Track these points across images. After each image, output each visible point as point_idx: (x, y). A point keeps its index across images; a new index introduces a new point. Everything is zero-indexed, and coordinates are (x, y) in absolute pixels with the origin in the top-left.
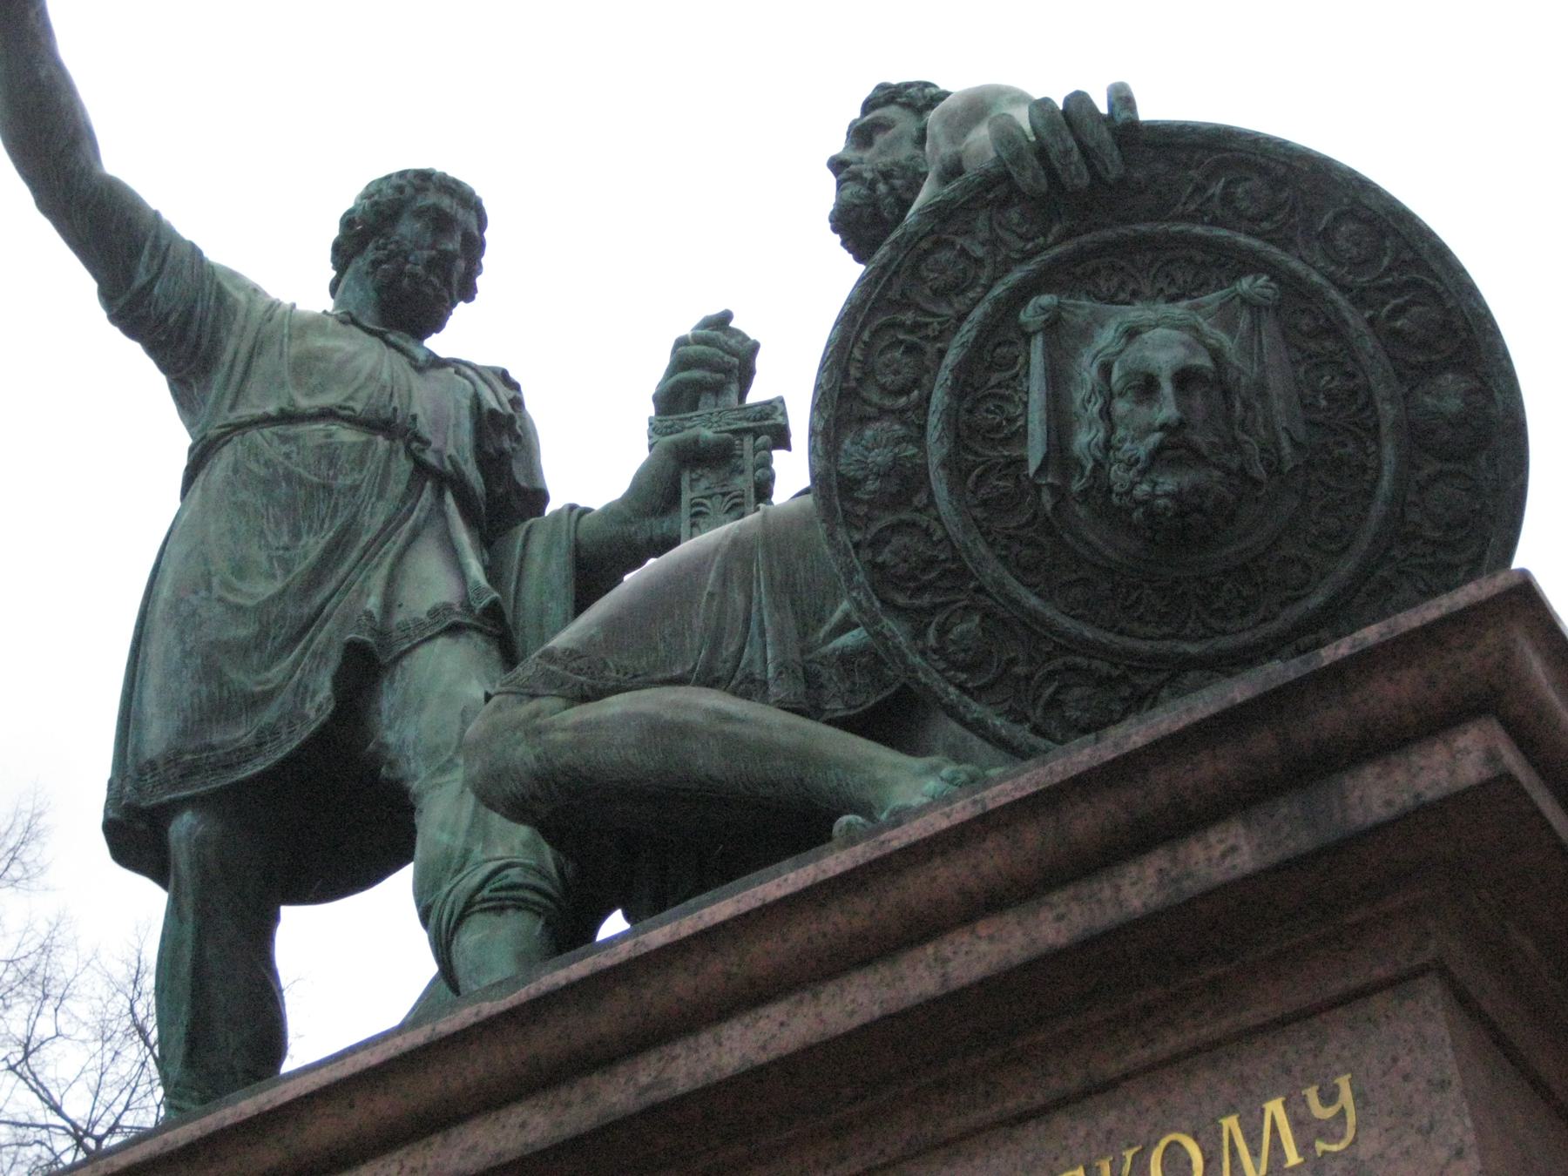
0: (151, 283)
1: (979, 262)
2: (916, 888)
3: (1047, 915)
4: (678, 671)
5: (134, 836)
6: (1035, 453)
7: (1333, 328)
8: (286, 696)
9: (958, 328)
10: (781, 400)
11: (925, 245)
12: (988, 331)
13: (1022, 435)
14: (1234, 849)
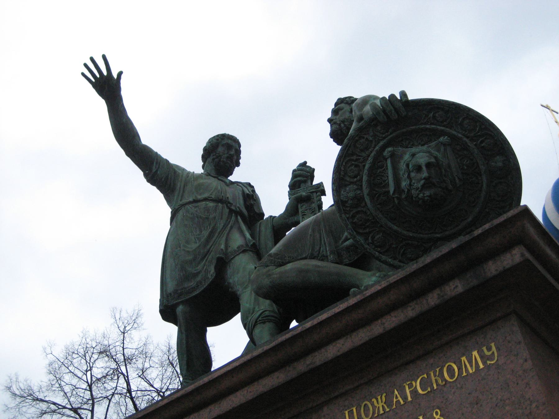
0: (157, 171)
1: (371, 141)
3: (409, 309)
4: (304, 256)
5: (168, 313)
6: (392, 189)
9: (368, 159)
10: (322, 183)
11: (357, 138)
12: (375, 158)
13: (388, 185)
14: (457, 286)
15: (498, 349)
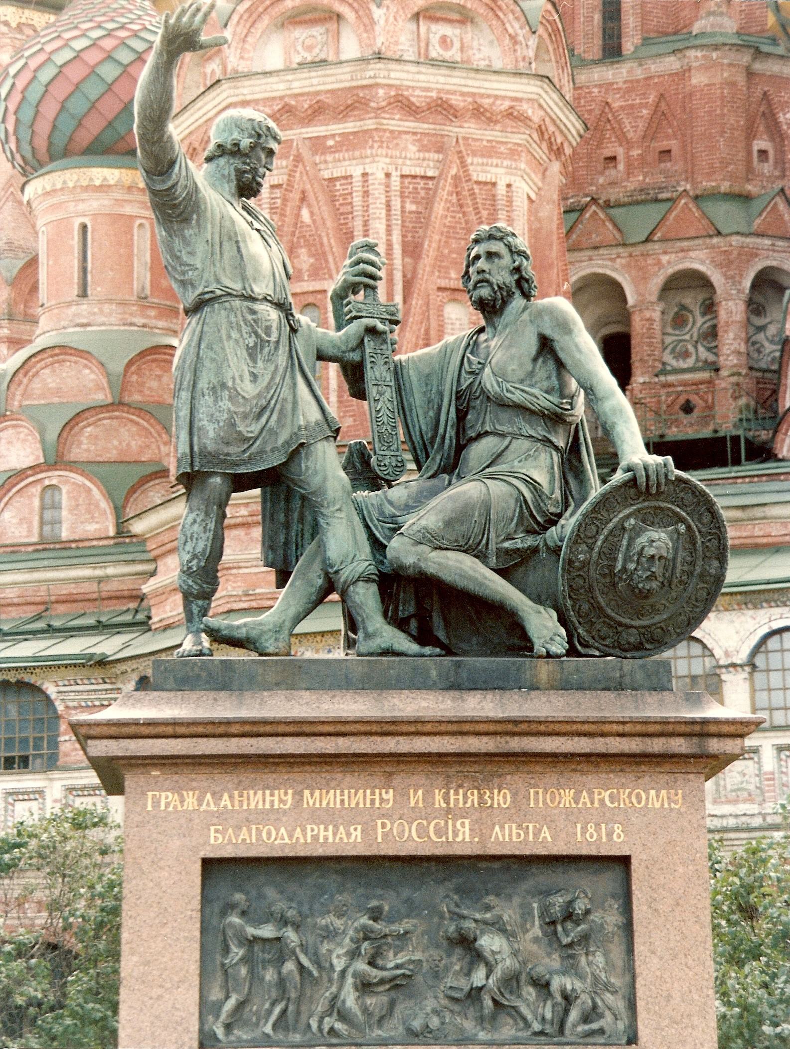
2: (607, 728)
6: (619, 566)
7: (693, 542)
15: (684, 798)
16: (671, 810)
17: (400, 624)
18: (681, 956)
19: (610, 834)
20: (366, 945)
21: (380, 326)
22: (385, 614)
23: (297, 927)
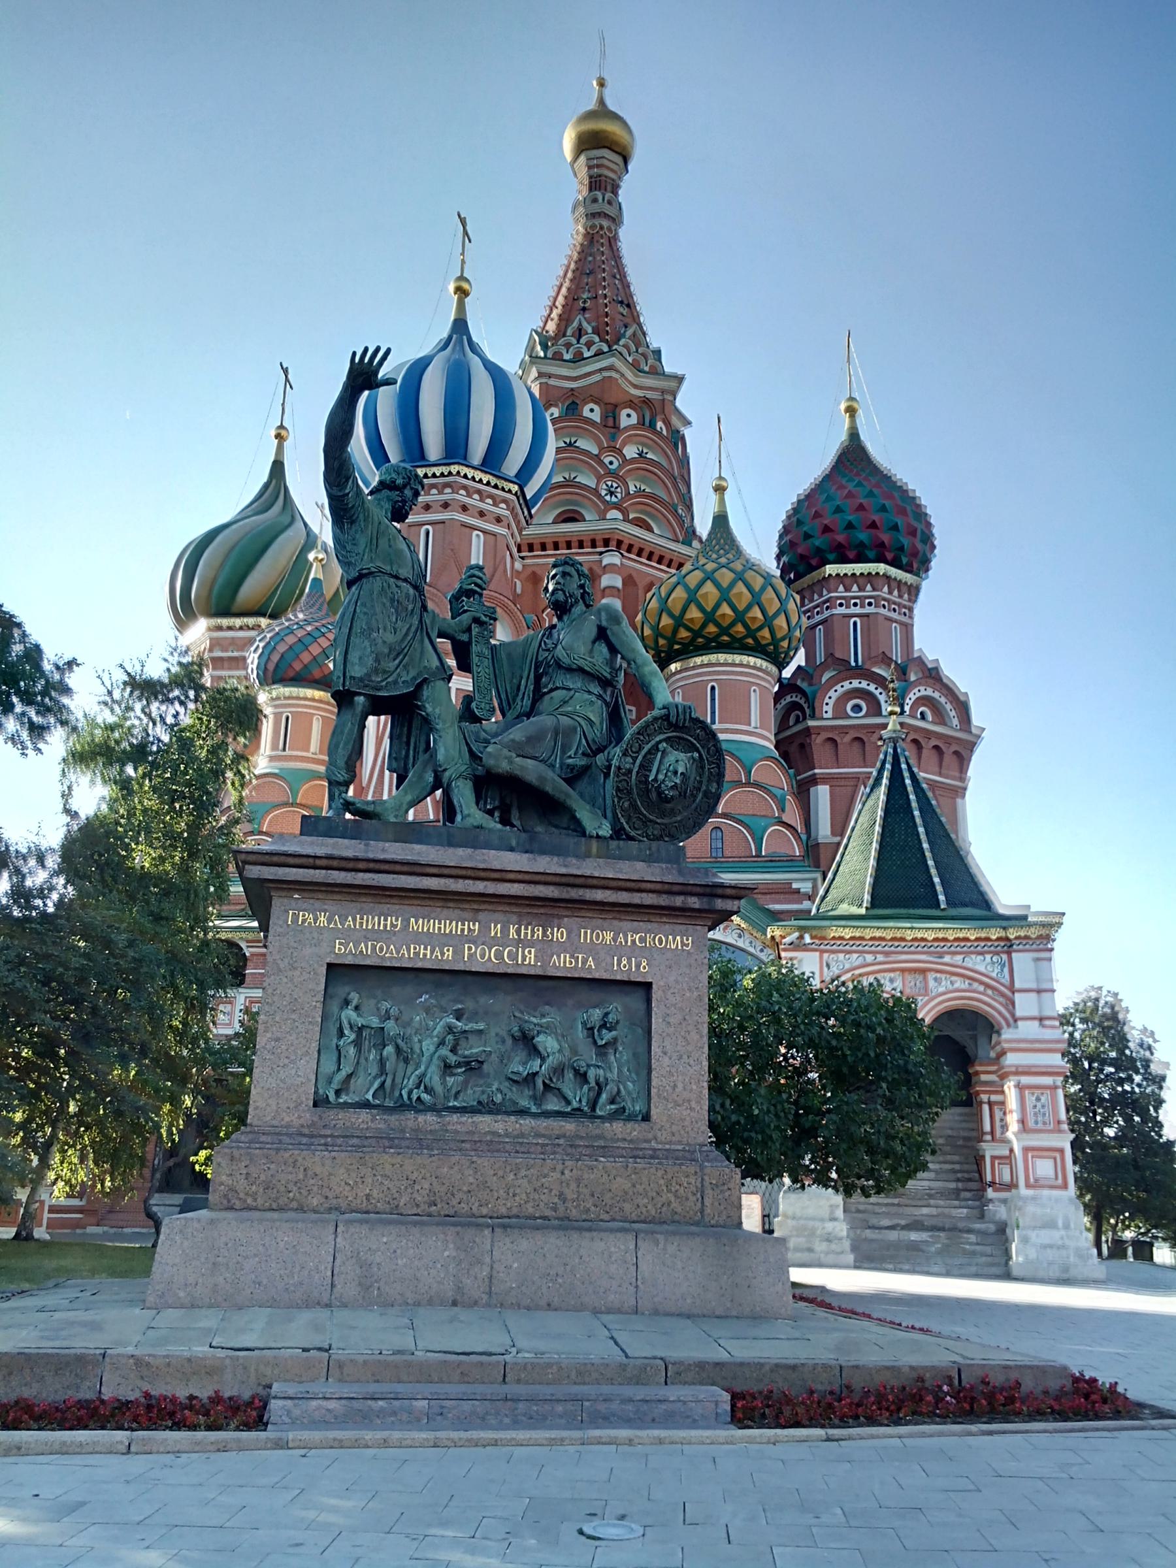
2: (644, 886)
7: (703, 768)
8: (395, 675)
16: (683, 950)
17: (490, 813)
18: (685, 1057)
19: (638, 966)
20: (450, 1037)
21: (483, 618)
22: (477, 804)
23: (397, 1019)
